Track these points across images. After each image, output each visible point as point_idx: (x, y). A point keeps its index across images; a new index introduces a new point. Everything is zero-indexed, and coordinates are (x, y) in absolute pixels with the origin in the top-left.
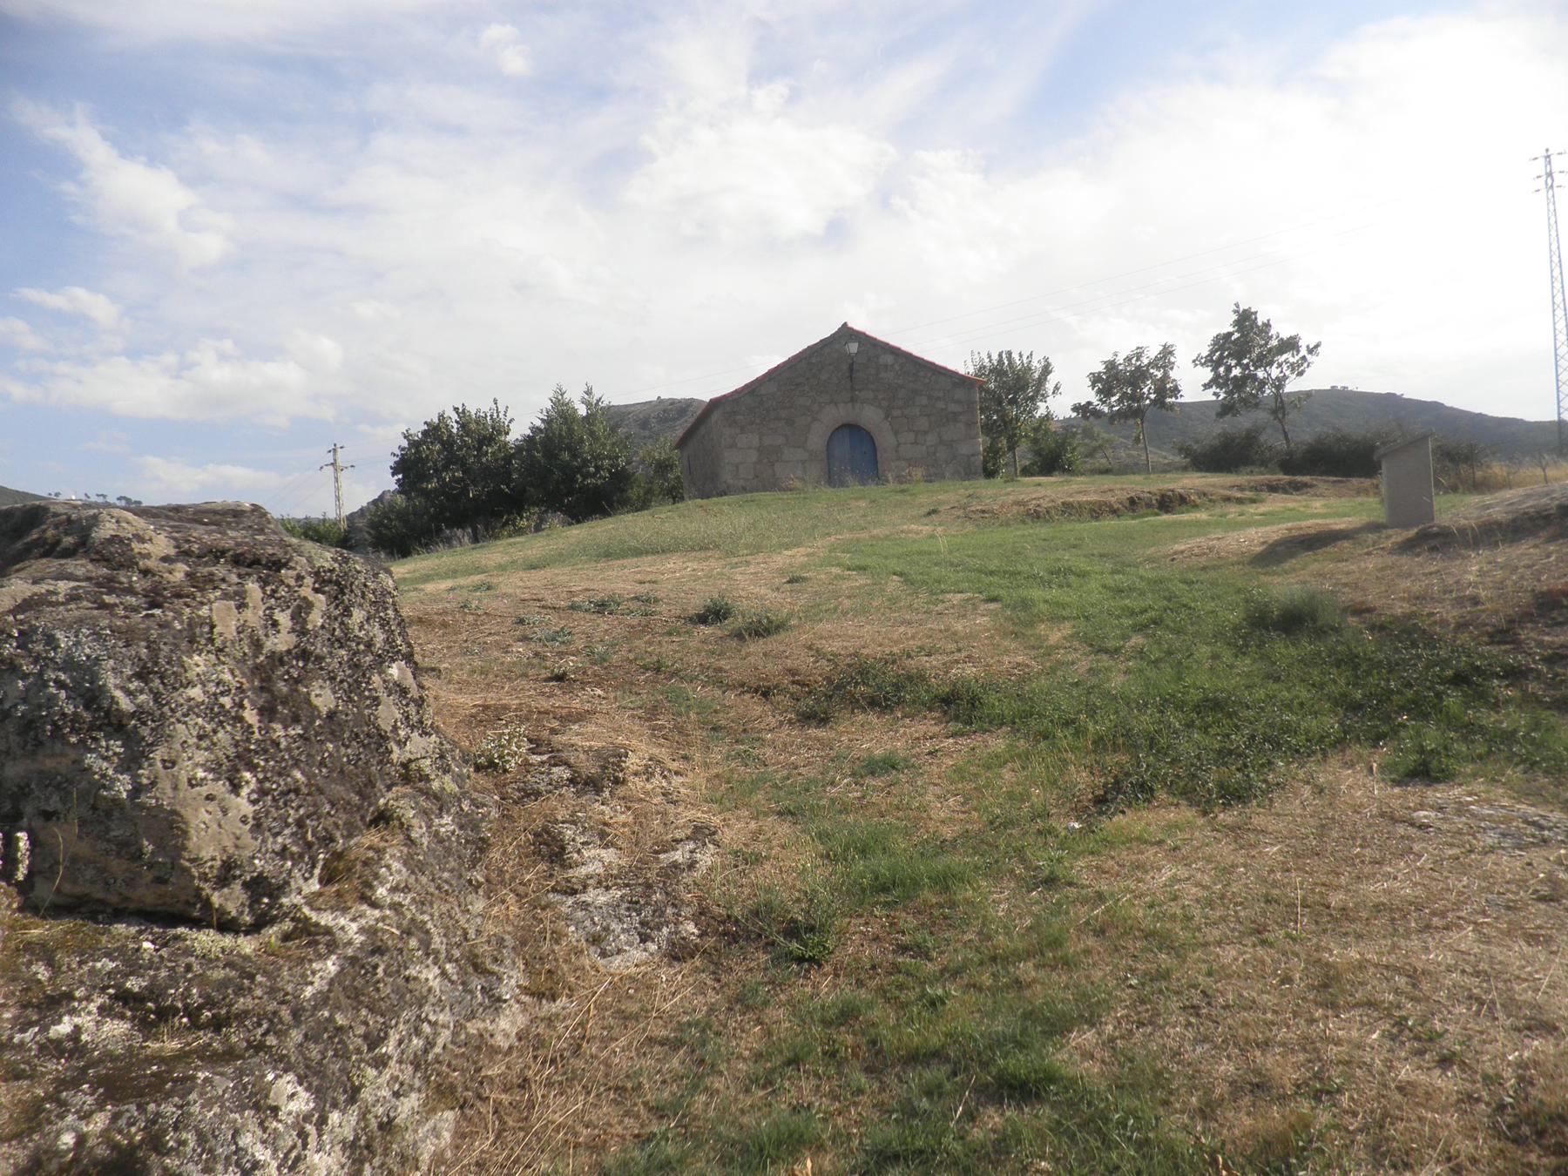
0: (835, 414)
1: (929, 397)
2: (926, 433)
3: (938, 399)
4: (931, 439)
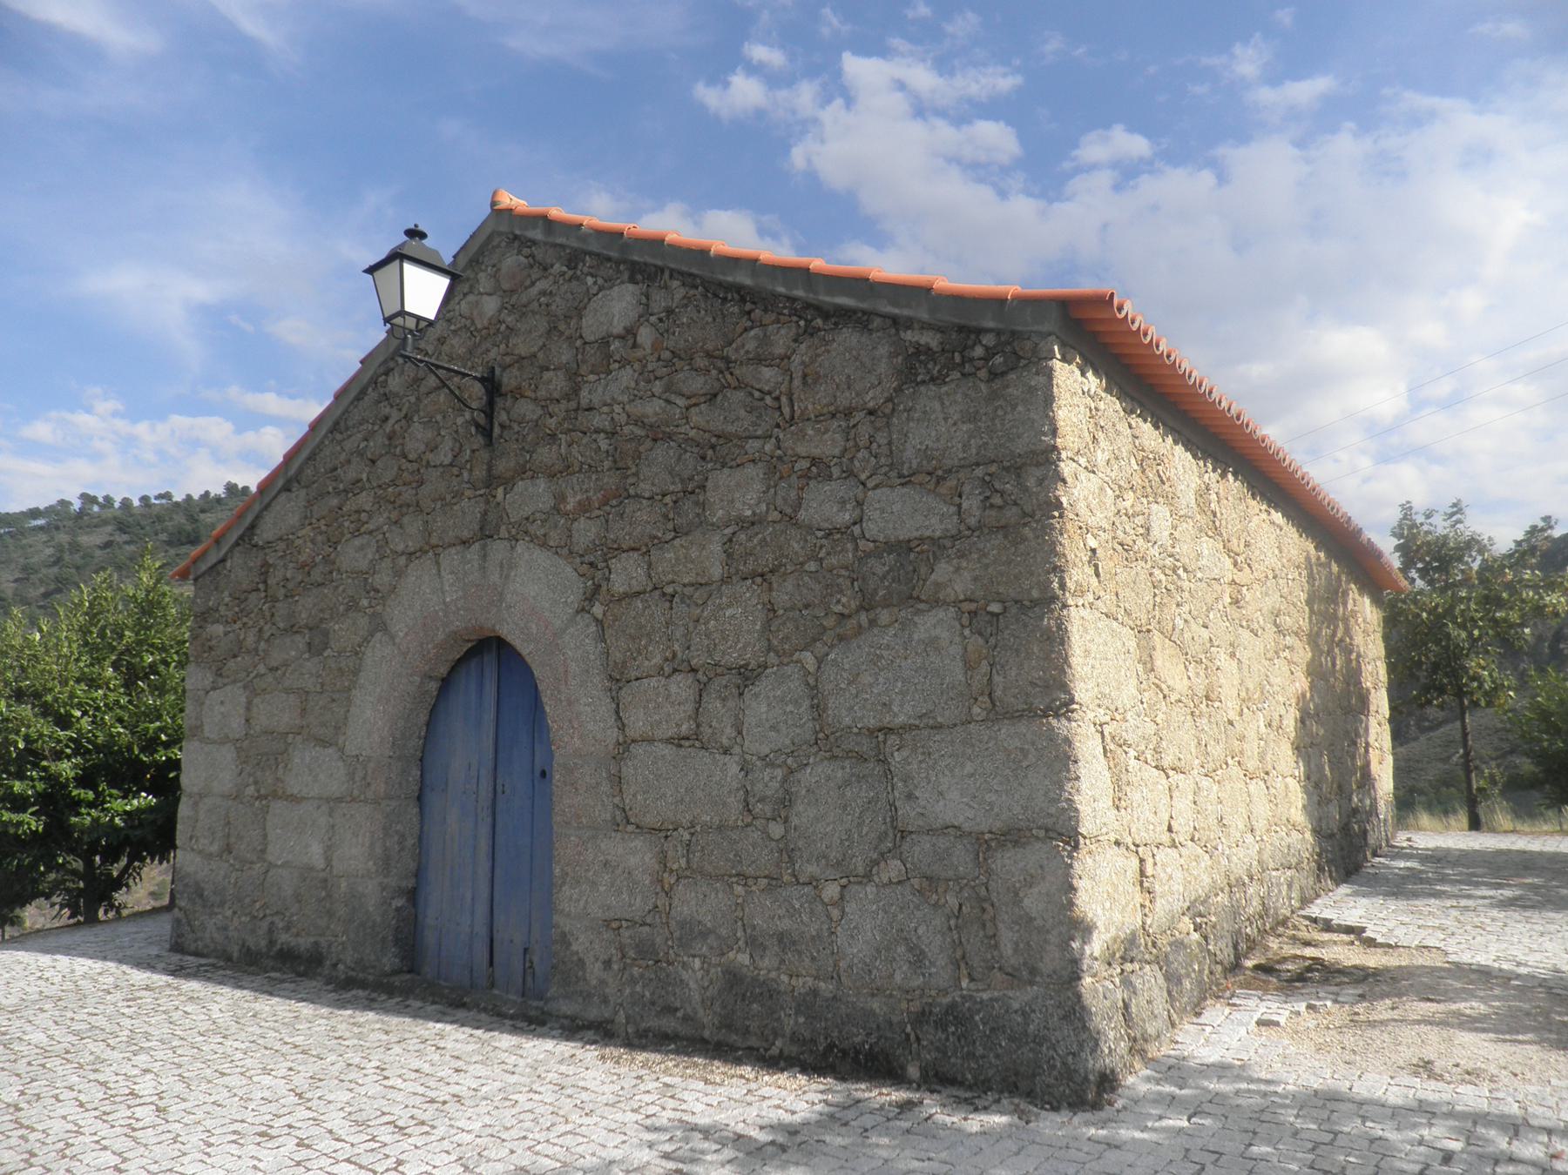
0: (430, 601)
1: (775, 468)
2: (747, 676)
3: (819, 468)
4: (771, 714)
